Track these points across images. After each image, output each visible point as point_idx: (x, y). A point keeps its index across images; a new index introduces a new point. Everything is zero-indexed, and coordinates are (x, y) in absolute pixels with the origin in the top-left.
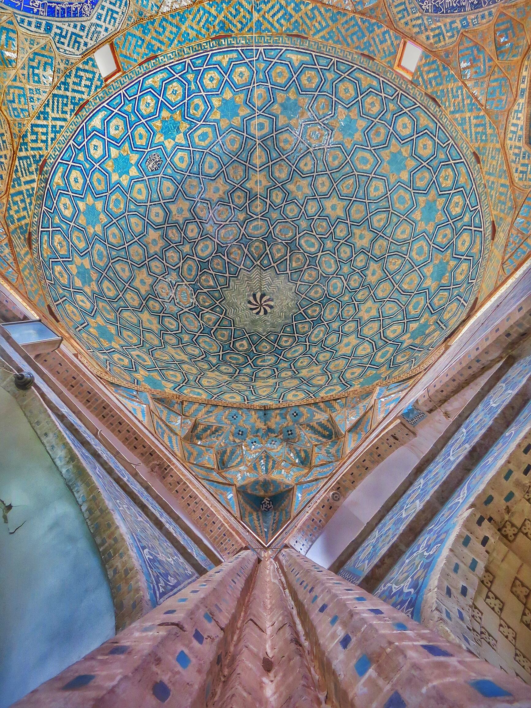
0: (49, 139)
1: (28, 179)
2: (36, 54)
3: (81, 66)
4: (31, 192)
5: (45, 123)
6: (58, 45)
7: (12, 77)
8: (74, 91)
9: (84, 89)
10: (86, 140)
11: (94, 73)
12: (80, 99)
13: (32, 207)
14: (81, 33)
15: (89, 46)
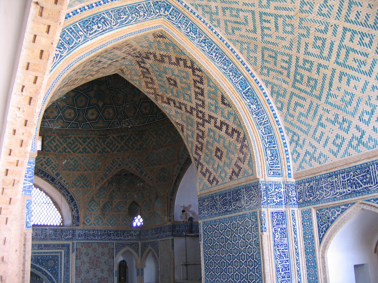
0: (90, 140)
1: (116, 142)
2: (69, 170)
3: (52, 151)
4: (120, 138)
5: (87, 148)
6: (57, 166)
7: (87, 172)
8: (62, 145)
9: (56, 141)
10: (72, 122)
11: (47, 144)
12: (61, 138)
13: (126, 134)
14: (44, 163)
15: (43, 156)
